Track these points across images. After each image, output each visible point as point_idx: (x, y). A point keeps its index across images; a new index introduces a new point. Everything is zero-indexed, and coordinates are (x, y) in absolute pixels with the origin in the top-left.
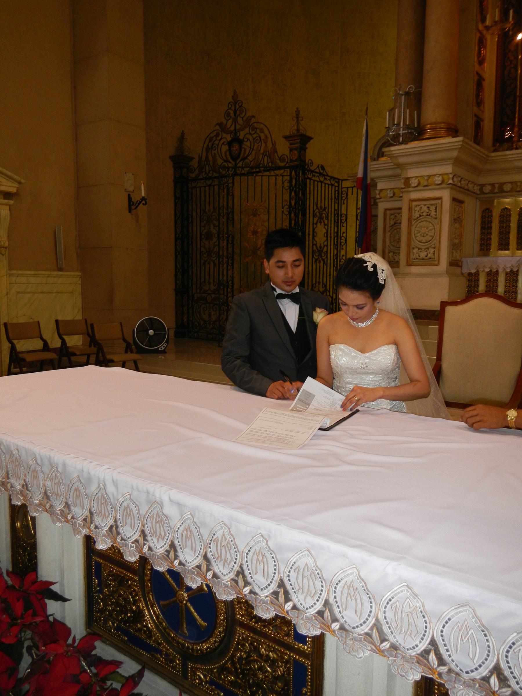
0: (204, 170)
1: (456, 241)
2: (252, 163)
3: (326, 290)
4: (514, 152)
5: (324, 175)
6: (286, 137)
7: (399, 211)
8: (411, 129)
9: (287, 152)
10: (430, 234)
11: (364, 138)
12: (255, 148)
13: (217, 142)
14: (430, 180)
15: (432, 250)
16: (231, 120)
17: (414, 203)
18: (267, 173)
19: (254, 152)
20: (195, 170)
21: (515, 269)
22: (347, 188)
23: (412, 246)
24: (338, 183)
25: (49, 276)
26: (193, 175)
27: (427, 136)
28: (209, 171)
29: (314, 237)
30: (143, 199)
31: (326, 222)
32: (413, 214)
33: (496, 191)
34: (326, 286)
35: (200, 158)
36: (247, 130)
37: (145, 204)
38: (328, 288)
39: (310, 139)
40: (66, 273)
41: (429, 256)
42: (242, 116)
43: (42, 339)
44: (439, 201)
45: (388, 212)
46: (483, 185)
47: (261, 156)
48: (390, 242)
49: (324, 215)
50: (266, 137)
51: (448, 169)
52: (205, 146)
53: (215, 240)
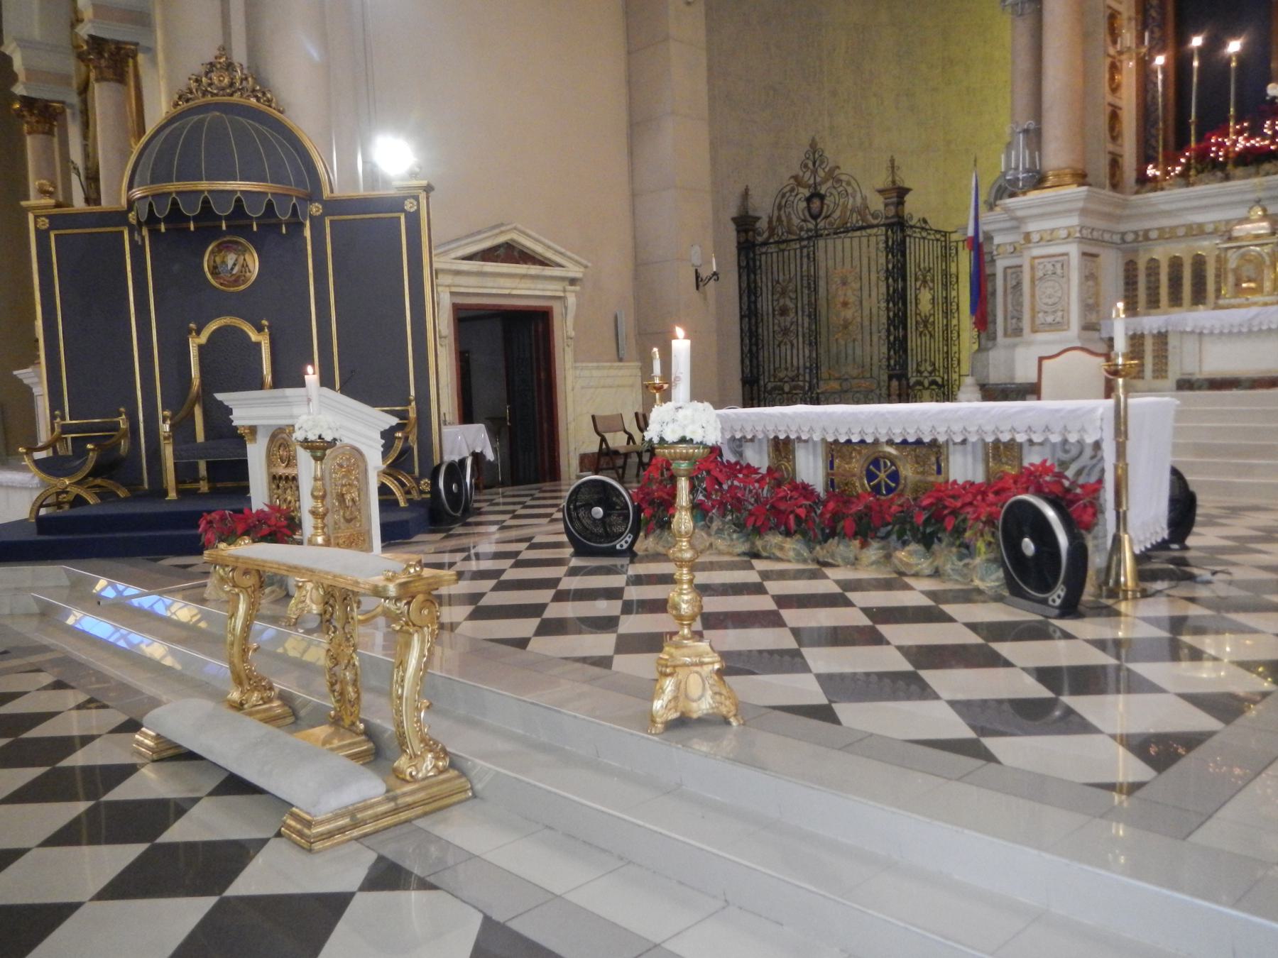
1: (1091, 301)
3: (934, 370)
4: (1159, 193)
5: (926, 230)
6: (881, 192)
7: (1019, 269)
8: (1032, 172)
9: (881, 207)
11: (973, 193)
12: (841, 203)
13: (791, 198)
14: (1055, 233)
15: (1060, 314)
18: (858, 233)
19: (840, 209)
20: (764, 233)
21: (1163, 330)
22: (957, 242)
23: (1037, 310)
24: (945, 236)
25: (611, 368)
26: (760, 239)
27: (1048, 184)
28: (783, 234)
30: (715, 274)
32: (1037, 273)
33: (1141, 239)
34: (934, 365)
35: (770, 222)
36: (829, 183)
39: (907, 191)
41: (1058, 319)
42: (823, 167)
43: (626, 432)
44: (1066, 257)
45: (1009, 271)
46: (1123, 234)
47: (848, 213)
48: (1013, 306)
49: (928, 278)
50: (855, 191)
51: (1074, 221)
53: (792, 315)
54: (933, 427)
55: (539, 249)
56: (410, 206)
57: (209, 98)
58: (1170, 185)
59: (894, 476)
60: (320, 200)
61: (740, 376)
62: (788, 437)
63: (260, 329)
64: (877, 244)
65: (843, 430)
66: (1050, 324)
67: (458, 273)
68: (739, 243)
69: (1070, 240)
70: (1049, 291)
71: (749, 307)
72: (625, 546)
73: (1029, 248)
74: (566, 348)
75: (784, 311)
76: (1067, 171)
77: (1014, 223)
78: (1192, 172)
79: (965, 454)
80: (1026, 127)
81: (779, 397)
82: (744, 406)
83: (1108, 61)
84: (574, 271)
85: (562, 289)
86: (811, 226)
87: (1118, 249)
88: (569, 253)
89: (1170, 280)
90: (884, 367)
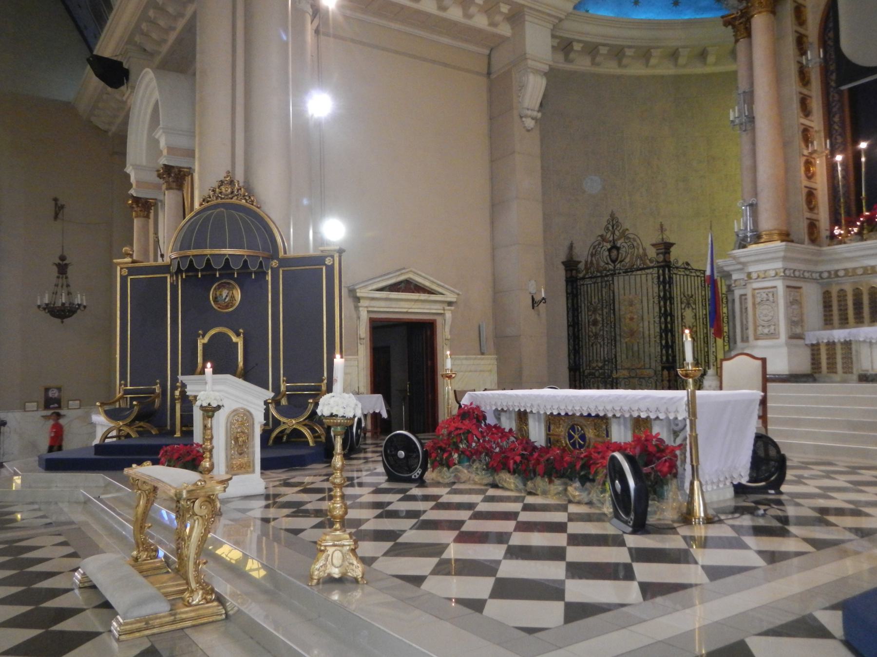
0: (589, 271)
2: (628, 265)
6: (653, 245)
9: (654, 255)
10: (770, 314)
11: (710, 246)
13: (599, 249)
15: (773, 327)
16: (610, 233)
17: (757, 291)
18: (639, 272)
19: (629, 256)
21: (848, 339)
26: (581, 275)
29: (682, 319)
30: (543, 299)
31: (694, 307)
33: (833, 276)
35: (586, 262)
36: (622, 240)
37: (545, 303)
38: (700, 361)
39: (672, 245)
40: (487, 356)
41: (772, 331)
42: (618, 229)
44: (775, 289)
46: (821, 273)
47: (634, 259)
49: (691, 302)
50: (638, 244)
51: (779, 265)
52: (590, 252)
54: (596, 406)
55: (427, 284)
56: (328, 261)
57: (219, 201)
58: (851, 240)
59: (583, 437)
60: (277, 258)
61: (567, 365)
62: (525, 410)
63: (238, 335)
64: (653, 279)
65: (549, 407)
66: (767, 334)
67: (373, 299)
68: (566, 278)
69: (777, 277)
70: (765, 312)
71: (573, 320)
72: (417, 476)
73: (750, 283)
74: (445, 346)
75: (595, 323)
76: (776, 232)
77: (739, 266)
78: (865, 232)
79: (619, 424)
80: (750, 202)
81: (593, 380)
82: (570, 387)
83: (803, 159)
84: (451, 298)
85: (442, 308)
86: (611, 267)
87: (818, 283)
88: (446, 286)
89: (854, 304)
90: (659, 361)
